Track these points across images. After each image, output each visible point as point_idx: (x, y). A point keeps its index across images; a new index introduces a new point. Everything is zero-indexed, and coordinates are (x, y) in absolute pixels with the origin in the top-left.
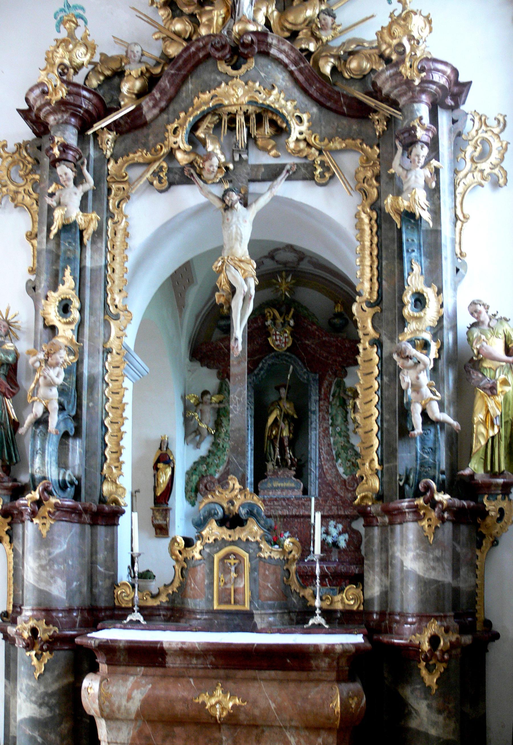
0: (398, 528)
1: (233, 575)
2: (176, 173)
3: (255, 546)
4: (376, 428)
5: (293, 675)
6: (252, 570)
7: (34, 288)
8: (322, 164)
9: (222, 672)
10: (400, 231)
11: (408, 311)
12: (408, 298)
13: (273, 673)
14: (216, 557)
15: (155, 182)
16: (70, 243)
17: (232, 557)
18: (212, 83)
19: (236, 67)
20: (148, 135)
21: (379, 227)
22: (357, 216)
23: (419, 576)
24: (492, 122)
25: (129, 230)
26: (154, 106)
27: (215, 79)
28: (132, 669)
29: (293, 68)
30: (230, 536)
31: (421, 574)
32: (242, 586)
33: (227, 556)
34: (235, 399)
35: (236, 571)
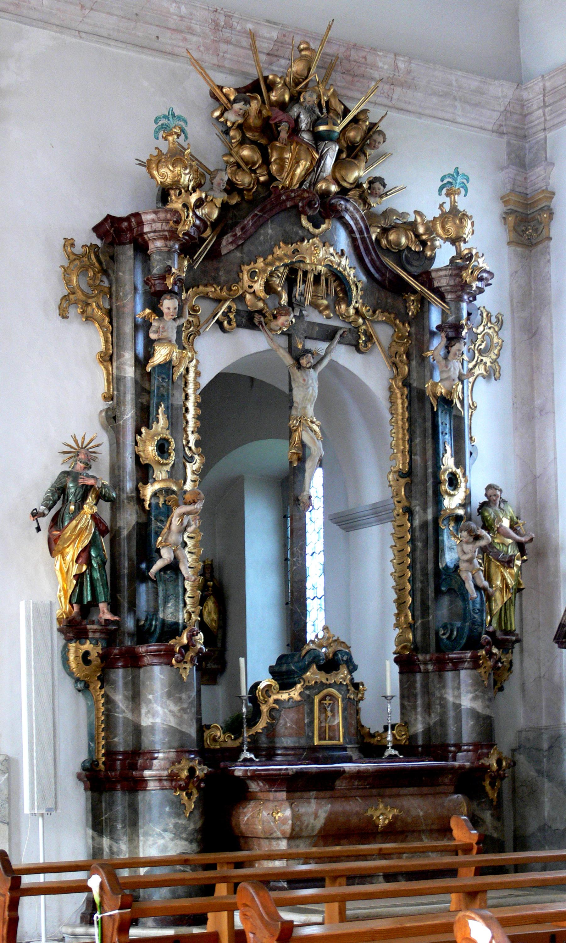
0: (449, 675)
1: (329, 714)
2: (243, 317)
3: (344, 688)
4: (409, 587)
5: (425, 790)
6: (344, 709)
7: (114, 418)
8: (366, 333)
9: (375, 791)
10: (435, 415)
11: (445, 487)
12: (445, 477)
13: (411, 789)
14: (317, 699)
15: (225, 323)
16: (163, 378)
17: (328, 698)
18: (293, 236)
19: (316, 226)
20: (217, 270)
21: (410, 404)
22: (390, 388)
23: (478, 713)
24: (494, 320)
25: (200, 369)
26: (232, 243)
27: (297, 233)
28: (306, 795)
29: (358, 236)
30: (327, 680)
31: (480, 711)
32: (336, 723)
33: (324, 698)
34: (297, 552)
35: (332, 711)
